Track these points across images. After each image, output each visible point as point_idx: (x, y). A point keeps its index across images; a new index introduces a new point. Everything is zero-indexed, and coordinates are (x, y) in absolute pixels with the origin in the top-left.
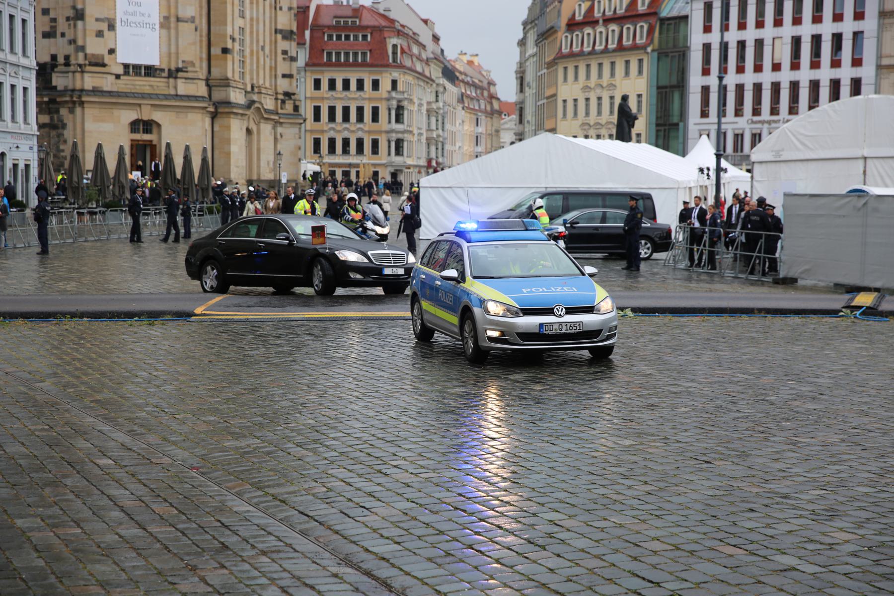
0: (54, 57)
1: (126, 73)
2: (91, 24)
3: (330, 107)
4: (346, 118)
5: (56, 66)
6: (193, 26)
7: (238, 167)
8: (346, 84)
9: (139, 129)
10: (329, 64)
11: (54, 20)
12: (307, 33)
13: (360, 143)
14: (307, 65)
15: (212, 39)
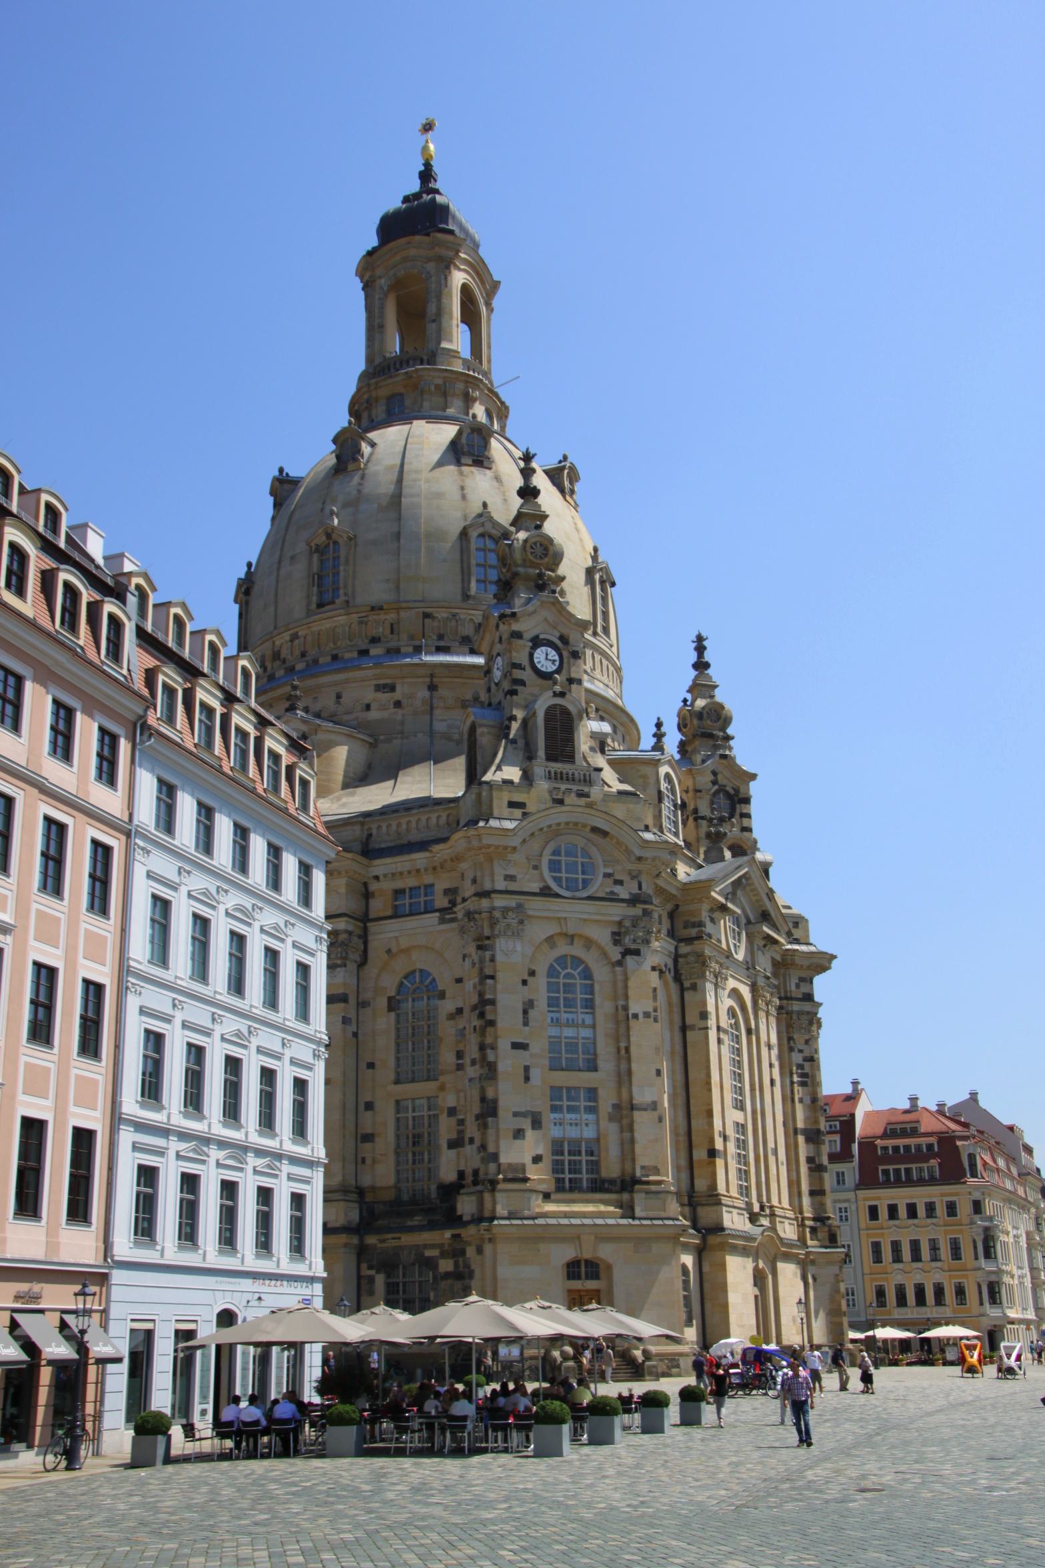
0: (461, 1174)
1: (560, 1187)
2: (505, 1121)
3: (892, 1242)
4: (916, 1257)
5: (463, 1186)
6: (655, 1115)
7: (743, 1326)
8: (912, 1211)
9: (579, 1273)
10: (887, 1184)
11: (461, 1122)
12: (855, 1148)
13: (939, 1291)
14: (858, 1187)
15: (693, 1138)
